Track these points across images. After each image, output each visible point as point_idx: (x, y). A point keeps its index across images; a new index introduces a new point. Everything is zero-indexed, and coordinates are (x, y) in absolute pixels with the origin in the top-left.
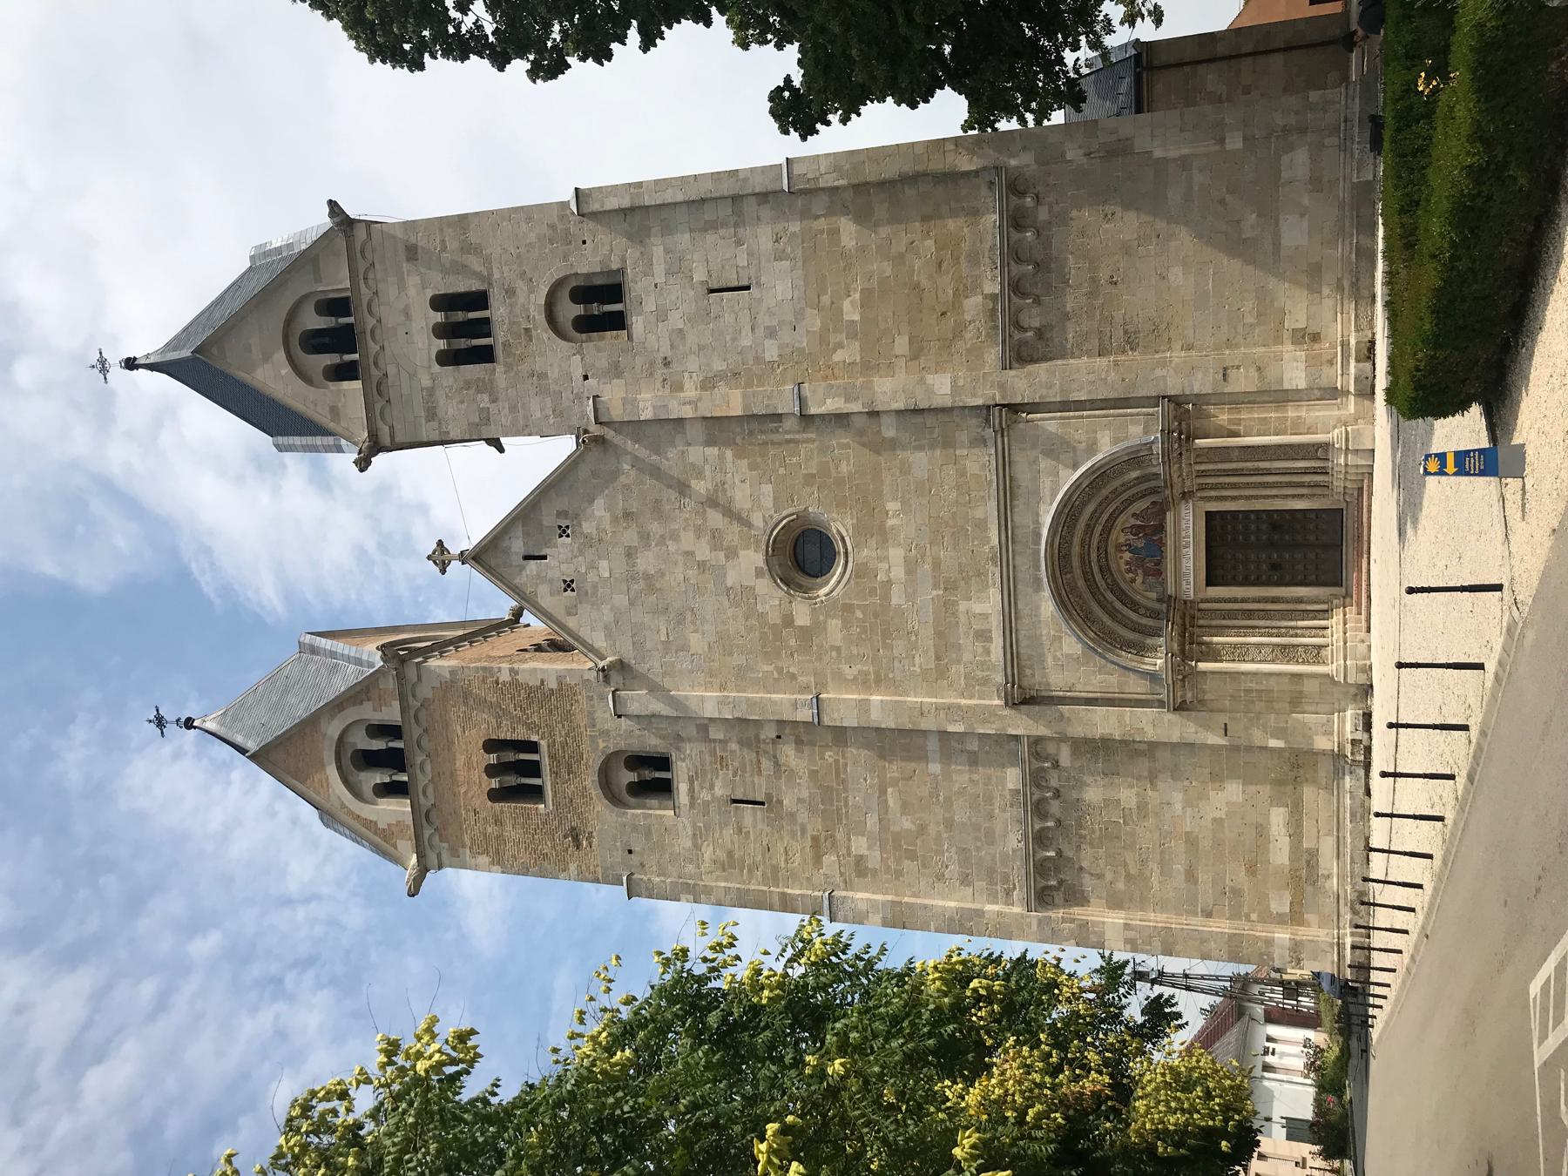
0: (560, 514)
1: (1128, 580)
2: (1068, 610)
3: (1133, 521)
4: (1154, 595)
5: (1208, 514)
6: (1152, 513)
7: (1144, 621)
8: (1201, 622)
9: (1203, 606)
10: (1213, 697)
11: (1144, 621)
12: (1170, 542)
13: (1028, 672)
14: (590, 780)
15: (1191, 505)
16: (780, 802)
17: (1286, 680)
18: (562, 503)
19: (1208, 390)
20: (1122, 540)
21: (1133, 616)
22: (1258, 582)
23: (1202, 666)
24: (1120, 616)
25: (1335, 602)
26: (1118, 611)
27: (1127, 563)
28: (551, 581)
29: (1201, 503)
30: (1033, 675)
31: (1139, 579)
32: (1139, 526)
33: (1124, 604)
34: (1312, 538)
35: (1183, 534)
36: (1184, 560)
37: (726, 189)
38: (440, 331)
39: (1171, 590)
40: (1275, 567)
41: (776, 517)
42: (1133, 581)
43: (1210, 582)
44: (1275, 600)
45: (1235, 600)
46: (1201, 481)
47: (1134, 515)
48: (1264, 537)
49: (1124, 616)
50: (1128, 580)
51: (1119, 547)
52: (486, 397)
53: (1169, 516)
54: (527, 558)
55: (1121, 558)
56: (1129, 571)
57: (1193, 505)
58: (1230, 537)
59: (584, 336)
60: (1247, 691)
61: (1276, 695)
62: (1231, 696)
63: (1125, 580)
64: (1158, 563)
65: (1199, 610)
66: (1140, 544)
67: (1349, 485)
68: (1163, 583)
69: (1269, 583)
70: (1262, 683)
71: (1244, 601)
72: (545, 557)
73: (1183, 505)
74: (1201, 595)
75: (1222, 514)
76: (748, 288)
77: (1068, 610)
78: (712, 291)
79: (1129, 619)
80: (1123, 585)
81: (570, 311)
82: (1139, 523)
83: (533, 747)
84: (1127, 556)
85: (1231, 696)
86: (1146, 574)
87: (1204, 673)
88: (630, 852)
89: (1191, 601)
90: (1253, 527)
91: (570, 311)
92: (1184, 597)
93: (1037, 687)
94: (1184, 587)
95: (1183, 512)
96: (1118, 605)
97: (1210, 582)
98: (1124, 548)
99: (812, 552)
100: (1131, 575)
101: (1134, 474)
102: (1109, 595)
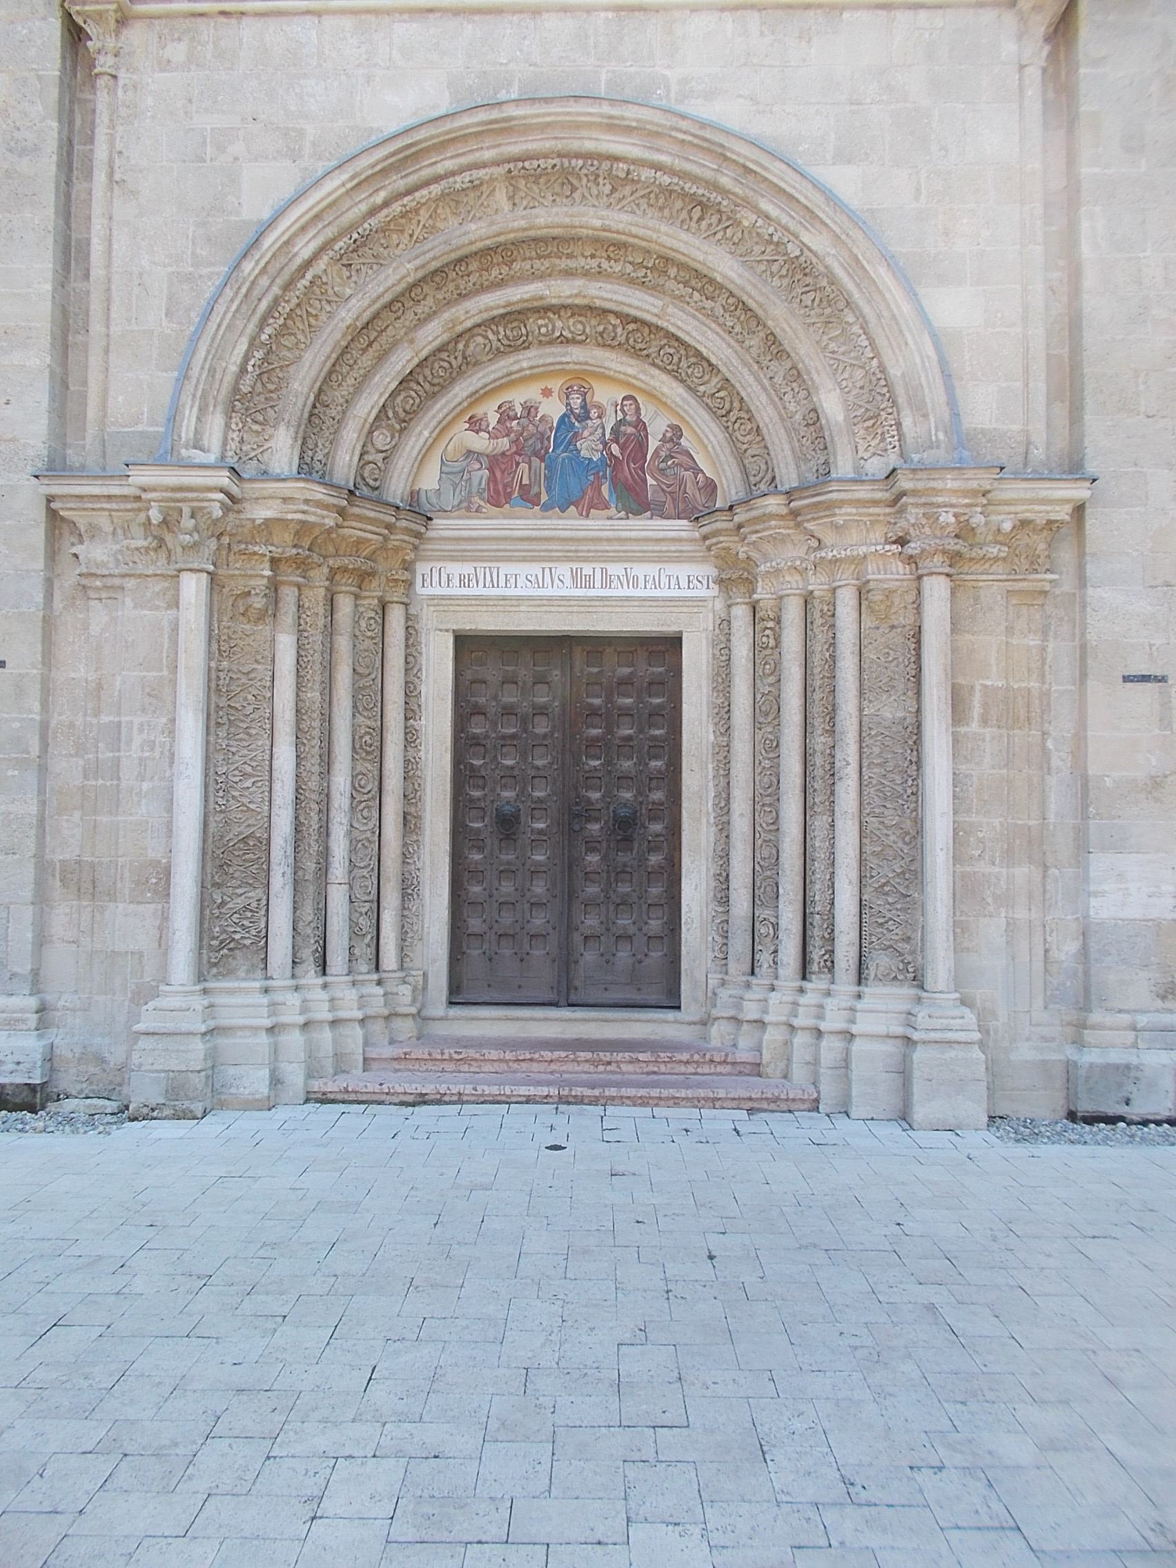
1: (479, 411)
2: (384, 172)
3: (657, 428)
4: (430, 480)
5: (673, 643)
6: (682, 482)
7: (351, 436)
8: (345, 605)
9: (396, 616)
10: (95, 629)
11: (351, 436)
12: (597, 525)
13: (177, 51)
15: (702, 592)
17: (154, 851)
19: (1097, 628)
20: (605, 395)
21: (367, 406)
22: (462, 775)
23: (193, 588)
24: (366, 361)
25: (405, 990)
26: (382, 357)
27: (530, 409)
29: (706, 621)
30: (166, 65)
31: (480, 442)
32: (642, 446)
33: (405, 381)
35: (615, 569)
36: (535, 569)
39: (443, 526)
40: (507, 825)
42: (476, 425)
44: (410, 823)
45: (410, 713)
46: (792, 614)
47: (677, 431)
48: (595, 795)
49: (367, 376)
50: (479, 411)
51: (579, 381)
53: (680, 527)
55: (547, 393)
56: (506, 415)
57: (704, 600)
58: (597, 701)
60: (116, 734)
61: (103, 819)
62: (100, 687)
63: (478, 397)
64: (529, 497)
65: (383, 606)
66: (588, 448)
67: (773, 1036)
68: (467, 508)
69: (461, 806)
70: (141, 777)
71: (411, 738)
73: (707, 570)
74: (428, 619)
75: (671, 684)
77: (384, 172)
79: (358, 389)
80: (461, 390)
82: (653, 444)
84: (553, 409)
85: (100, 687)
86: (495, 462)
87: (175, 603)
89: (410, 584)
90: (627, 765)
92: (422, 568)
93: (122, 74)
94: (457, 569)
95: (682, 571)
96: (402, 361)
97: (465, 644)
98: (576, 402)
100: (493, 419)
101: (832, 405)
102: (432, 334)
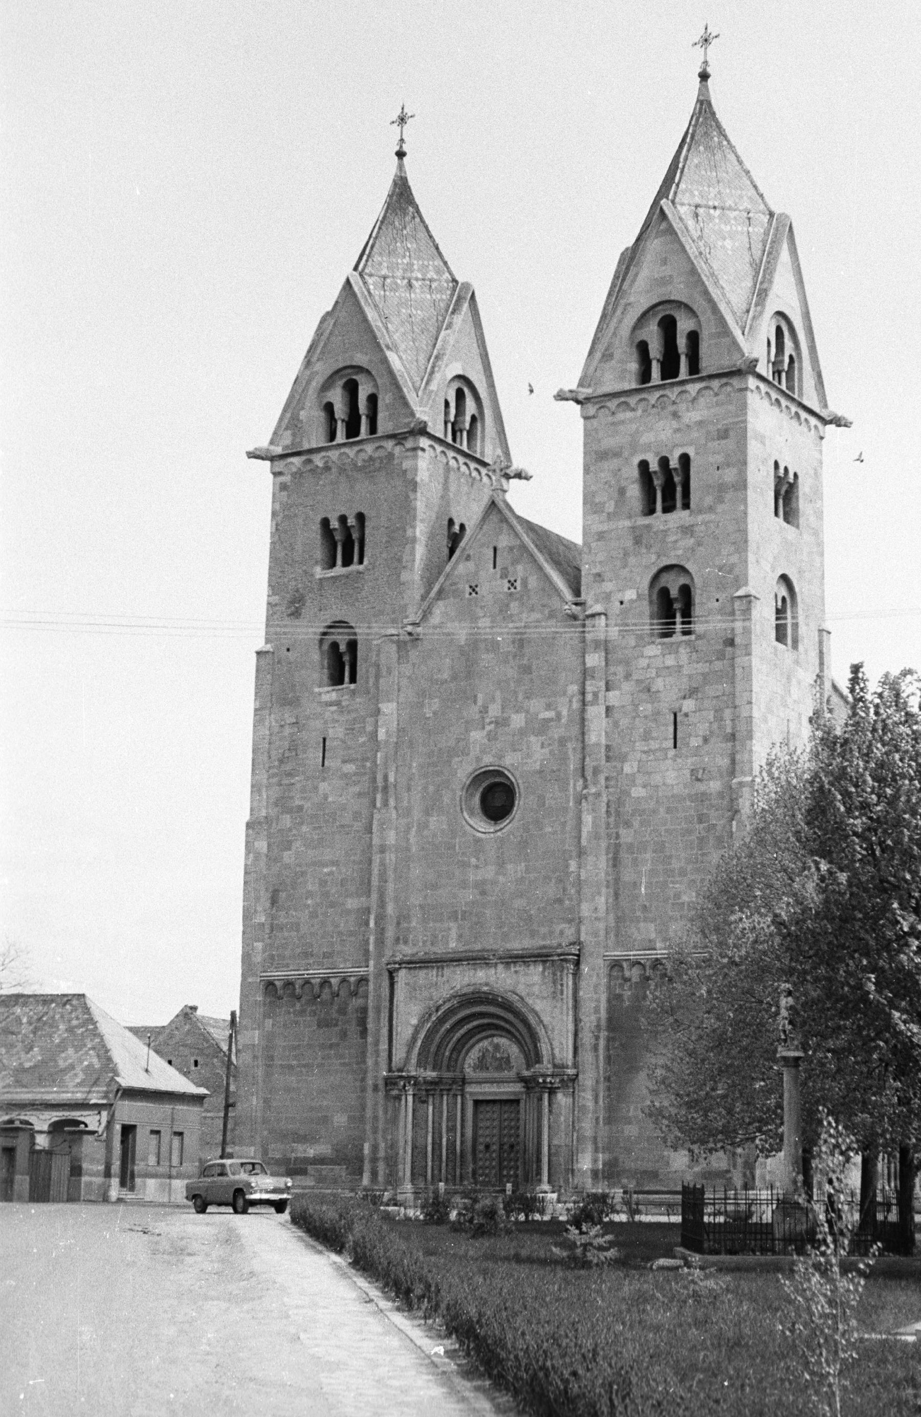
0: (525, 583)
14: (336, 612)
16: (324, 780)
18: (533, 582)
28: (476, 573)
34: (505, 1173)
37: (742, 727)
38: (664, 462)
41: (517, 774)
43: (477, 1103)
52: (611, 510)
54: (495, 549)
59: (655, 597)
72: (495, 567)
76: (675, 747)
78: (675, 715)
81: (674, 584)
83: (361, 562)
88: (288, 650)
91: (674, 584)
99: (498, 800)
